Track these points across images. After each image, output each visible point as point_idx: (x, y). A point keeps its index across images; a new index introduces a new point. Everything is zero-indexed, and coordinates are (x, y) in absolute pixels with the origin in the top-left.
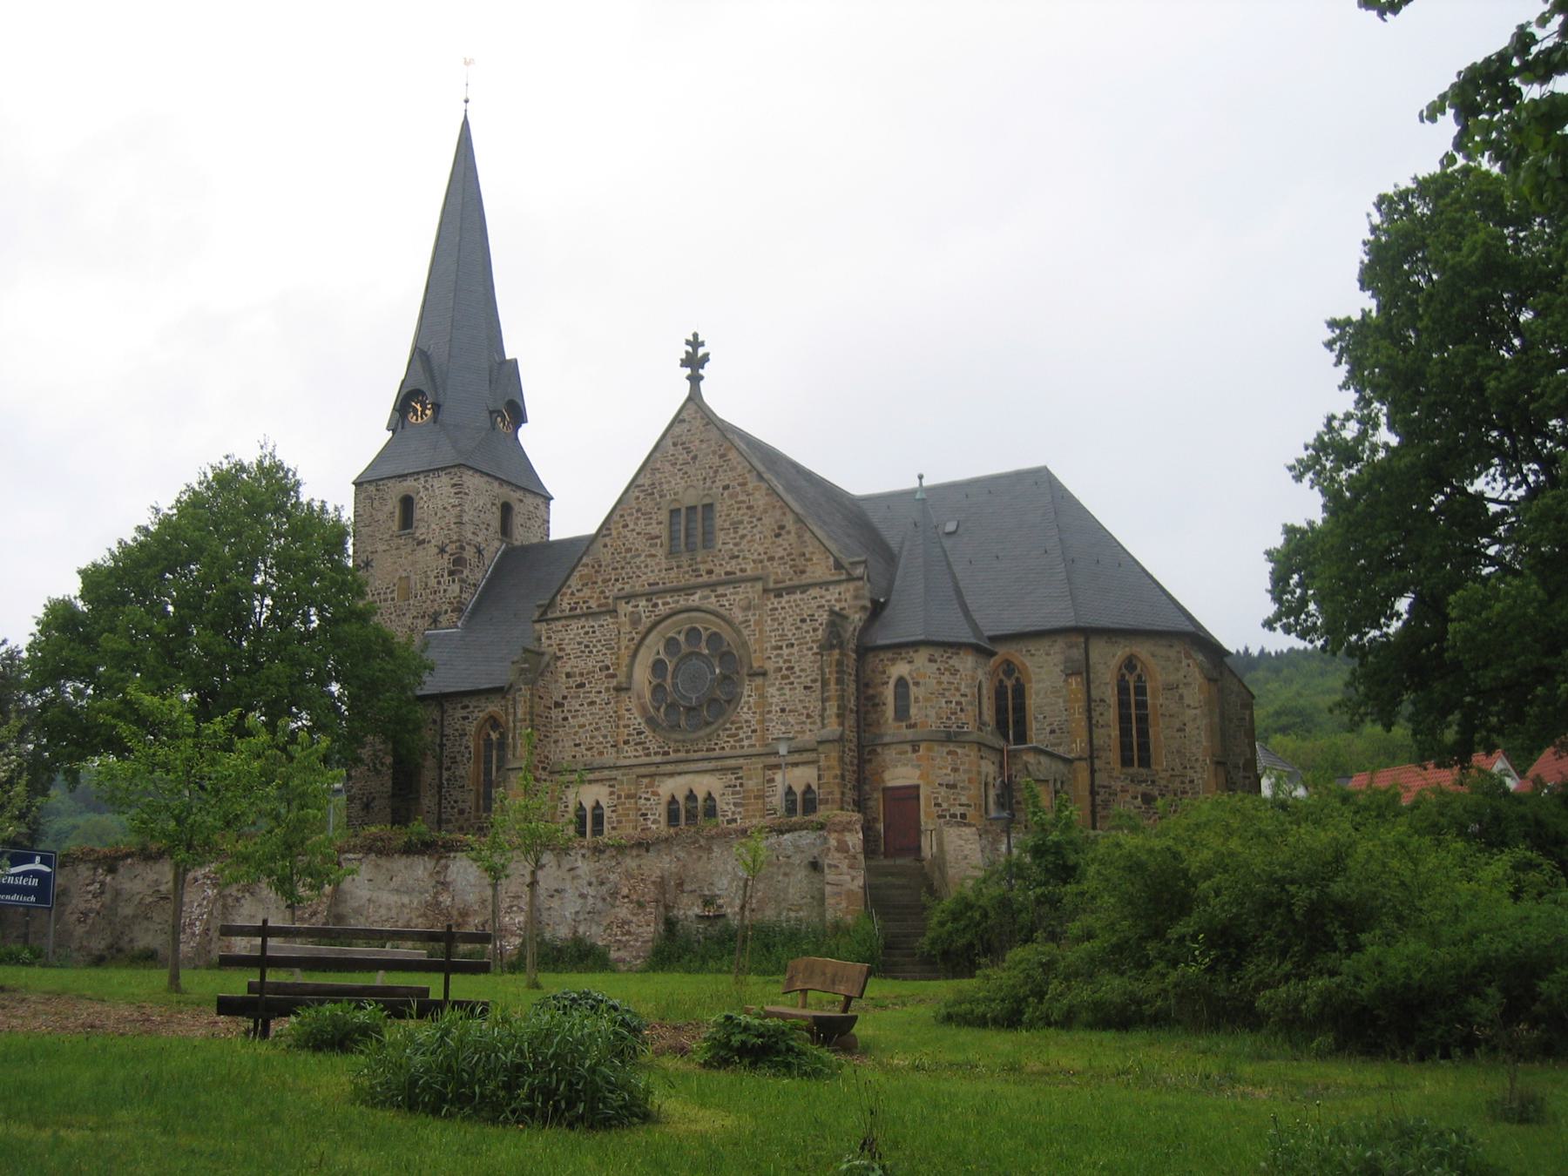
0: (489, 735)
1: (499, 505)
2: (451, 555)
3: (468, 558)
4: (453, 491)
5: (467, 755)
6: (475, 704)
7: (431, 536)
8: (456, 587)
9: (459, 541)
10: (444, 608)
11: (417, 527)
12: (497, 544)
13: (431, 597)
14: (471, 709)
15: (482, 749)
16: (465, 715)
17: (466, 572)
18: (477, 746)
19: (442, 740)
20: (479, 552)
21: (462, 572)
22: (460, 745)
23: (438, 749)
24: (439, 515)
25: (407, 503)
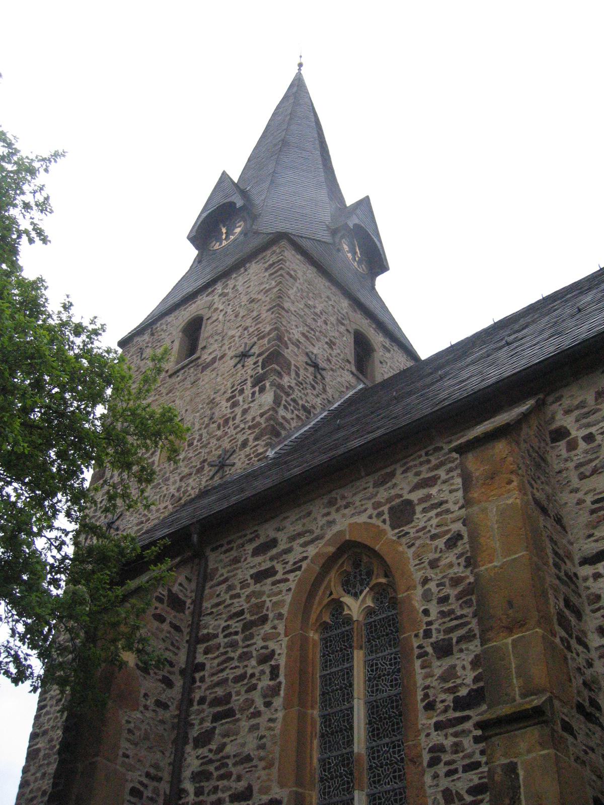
0: (337, 606)
1: (352, 331)
2: (259, 355)
3: (293, 362)
4: (267, 274)
5: (265, 682)
6: (299, 528)
7: (226, 347)
8: (268, 398)
9: (276, 329)
10: (241, 438)
11: (204, 348)
12: (347, 377)
13: (219, 433)
14: (282, 546)
15: (316, 654)
16: (267, 565)
17: (286, 381)
18: (300, 646)
19: (192, 654)
20: (316, 366)
21: (280, 375)
22: (245, 656)
23: (179, 682)
24: (241, 315)
25: (194, 329)
